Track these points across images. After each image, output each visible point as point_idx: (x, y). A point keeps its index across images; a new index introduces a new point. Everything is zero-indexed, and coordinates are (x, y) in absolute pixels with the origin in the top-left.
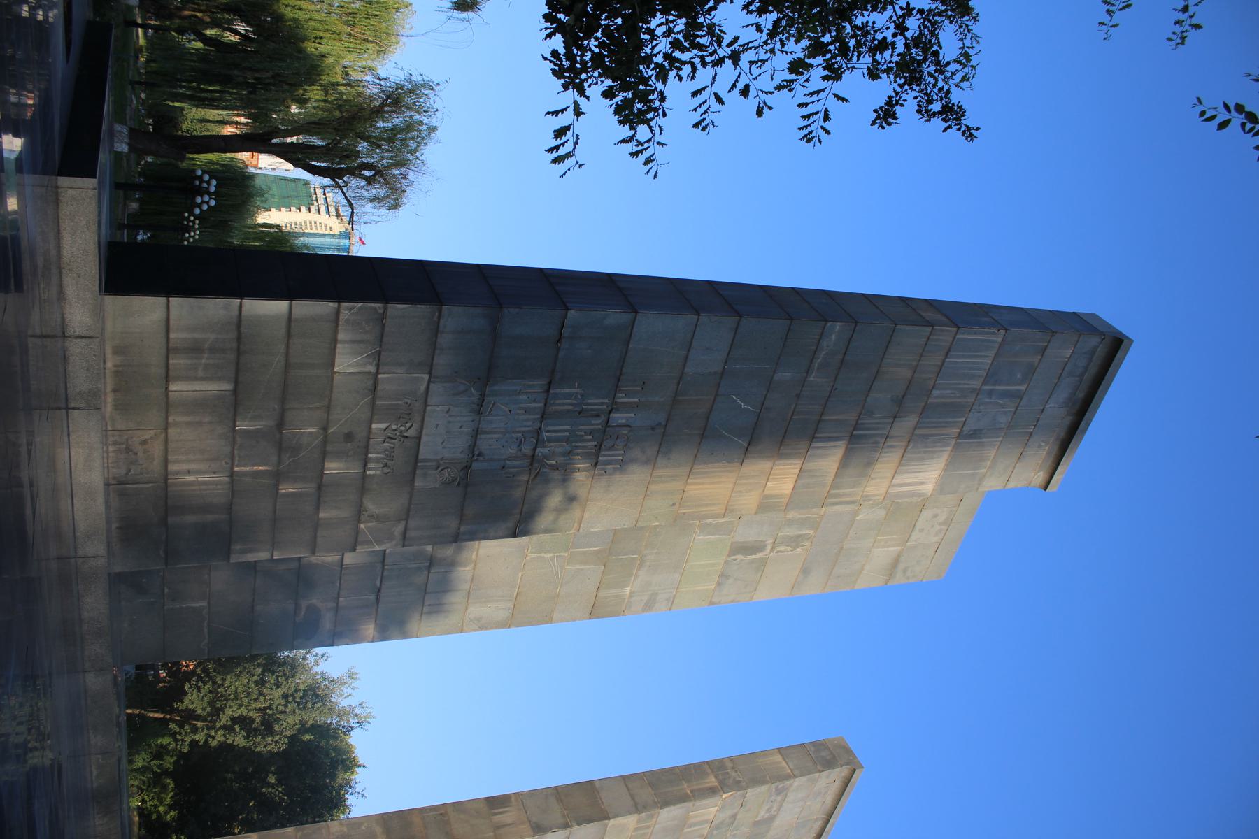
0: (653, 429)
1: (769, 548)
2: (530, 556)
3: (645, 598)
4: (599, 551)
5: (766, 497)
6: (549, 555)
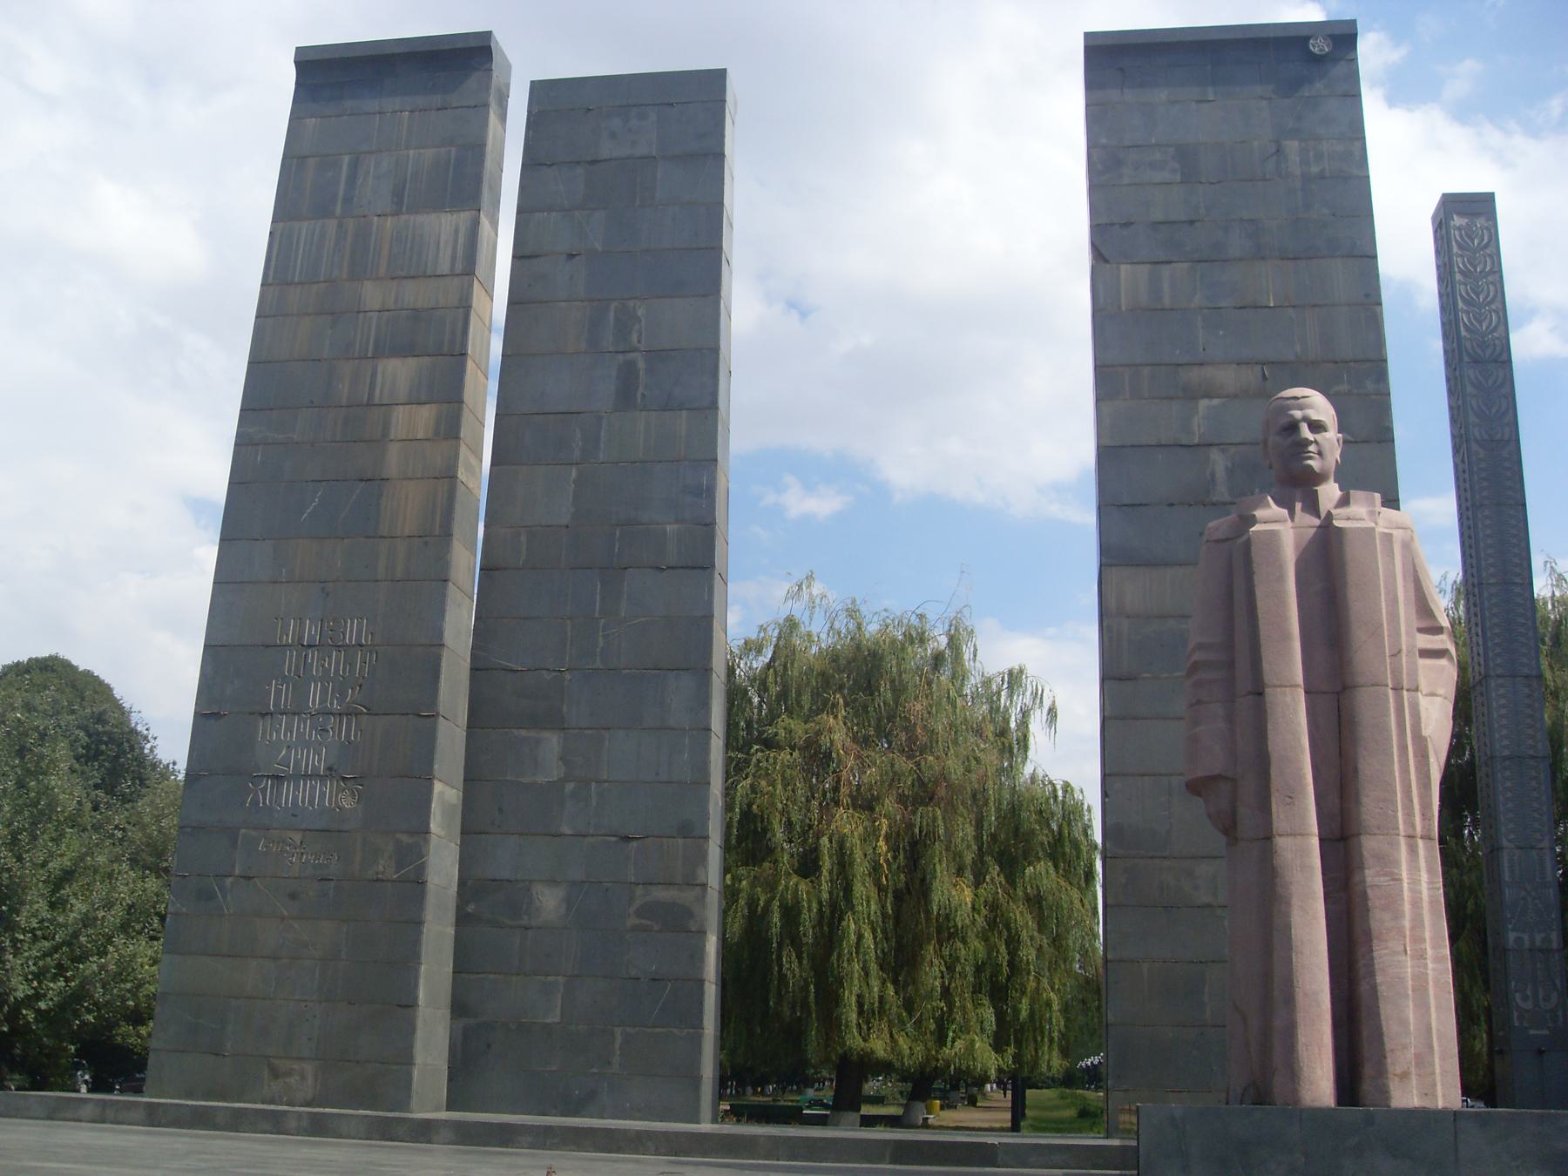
1: (632, 355)
2: (598, 664)
5: (437, 433)
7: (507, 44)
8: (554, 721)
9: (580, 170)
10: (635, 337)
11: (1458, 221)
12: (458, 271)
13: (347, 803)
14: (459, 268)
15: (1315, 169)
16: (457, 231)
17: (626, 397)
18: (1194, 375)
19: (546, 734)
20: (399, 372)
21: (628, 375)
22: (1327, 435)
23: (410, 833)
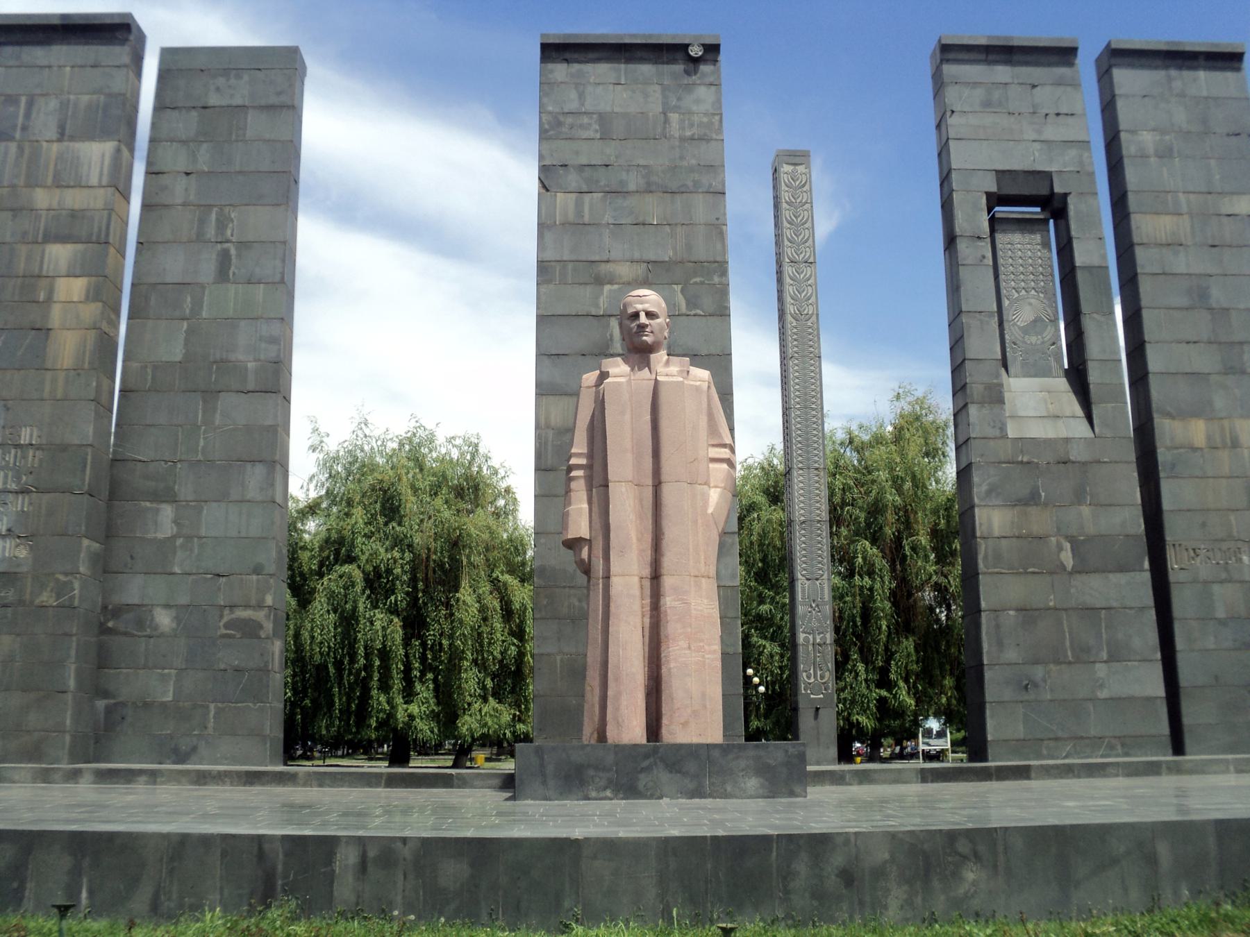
0: (8, 409)
1: (226, 245)
2: (200, 457)
3: (263, 345)
4: (205, 401)
6: (202, 443)
7: (145, 19)
8: (169, 496)
9: (194, 113)
10: (229, 232)
11: (787, 168)
12: (104, 183)
13: (23, 553)
14: (104, 182)
15: (688, 134)
16: (103, 156)
17: (223, 274)
18: (604, 268)
19: (164, 506)
20: (60, 254)
21: (225, 258)
22: (658, 321)
23: (66, 574)
